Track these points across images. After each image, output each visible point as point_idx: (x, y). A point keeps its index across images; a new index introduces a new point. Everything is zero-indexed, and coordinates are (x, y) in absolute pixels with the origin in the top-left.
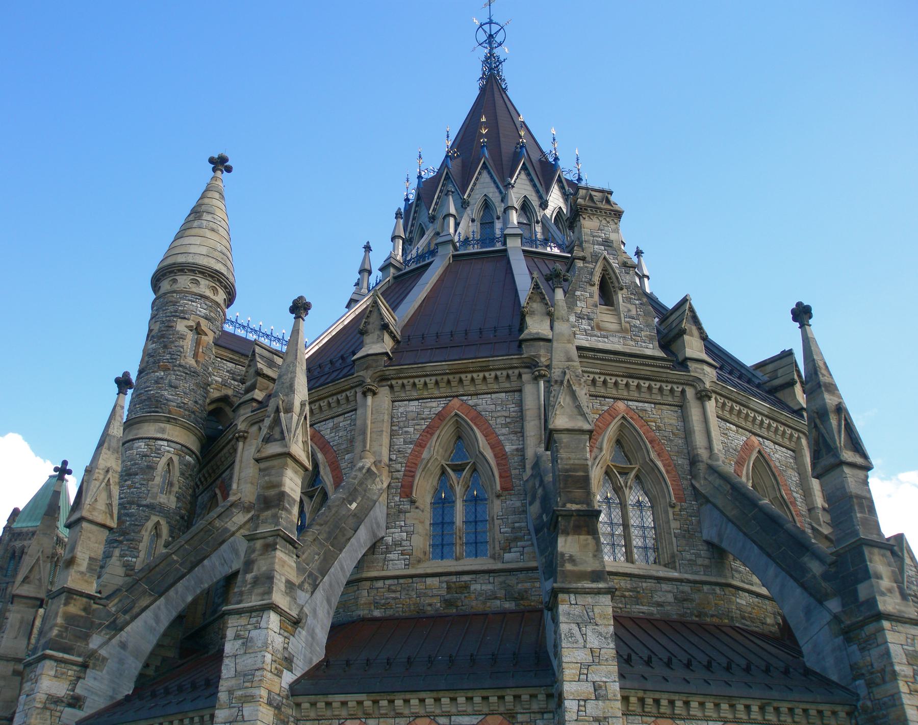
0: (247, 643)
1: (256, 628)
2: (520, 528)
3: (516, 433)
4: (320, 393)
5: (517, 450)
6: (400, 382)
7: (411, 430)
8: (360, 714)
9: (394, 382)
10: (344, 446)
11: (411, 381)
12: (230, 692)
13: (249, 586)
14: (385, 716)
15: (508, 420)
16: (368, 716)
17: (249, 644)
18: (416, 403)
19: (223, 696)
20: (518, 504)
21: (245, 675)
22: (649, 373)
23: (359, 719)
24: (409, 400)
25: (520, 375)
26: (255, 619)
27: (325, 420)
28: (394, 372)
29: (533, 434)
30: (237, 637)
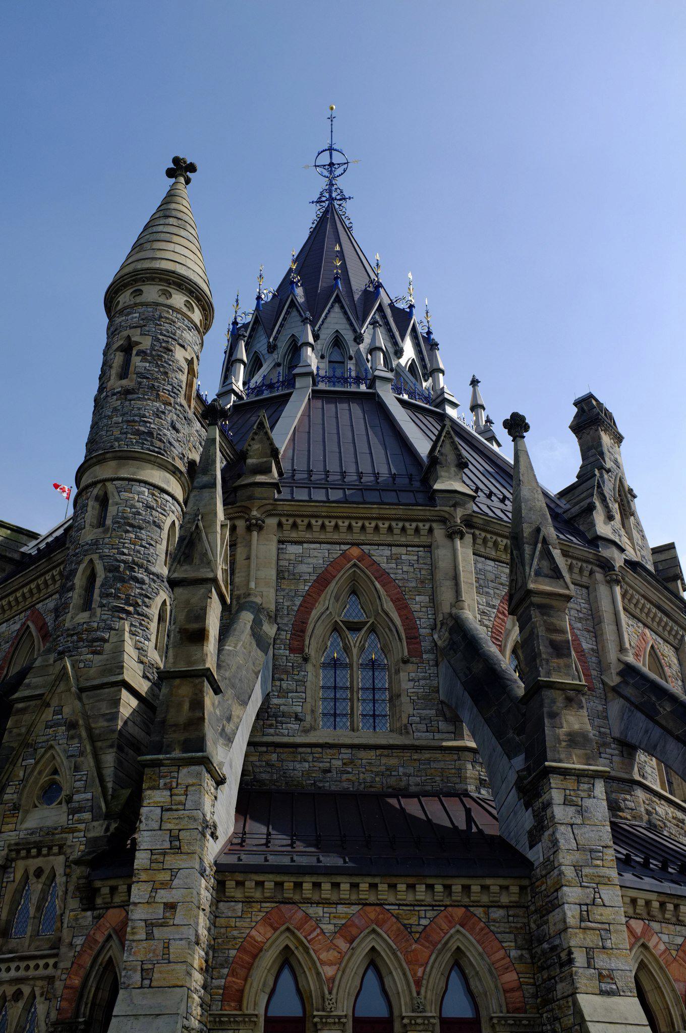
0: (581, 811)
1: (589, 797)
2: (605, 733)
3: (589, 631)
4: (382, 512)
5: (592, 650)
6: (483, 534)
7: (491, 592)
8: (645, 916)
9: (477, 532)
10: (414, 584)
11: (494, 538)
12: (577, 868)
13: (564, 744)
14: (667, 921)
15: (581, 615)
16: (652, 918)
17: (585, 814)
18: (491, 563)
19: (569, 872)
20: (600, 708)
21: (591, 851)
22: (669, 609)
23: (642, 919)
24: (487, 558)
25: (591, 573)
26: (586, 786)
27: (378, 545)
28: (481, 522)
29: (612, 639)
30: (567, 802)
